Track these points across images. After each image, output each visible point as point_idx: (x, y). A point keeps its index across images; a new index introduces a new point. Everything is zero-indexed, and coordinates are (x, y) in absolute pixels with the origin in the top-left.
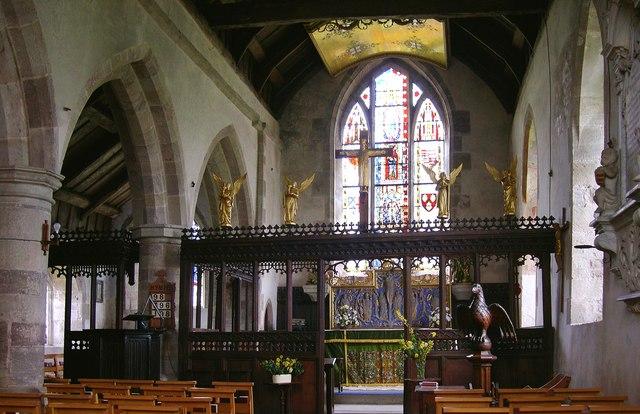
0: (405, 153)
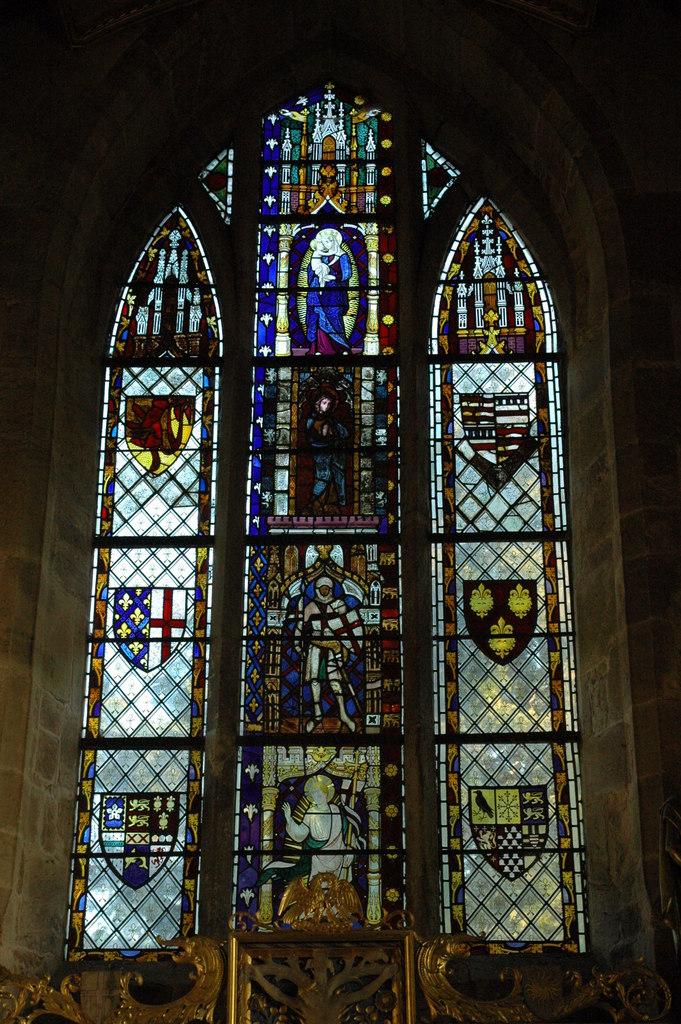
0: (383, 404)
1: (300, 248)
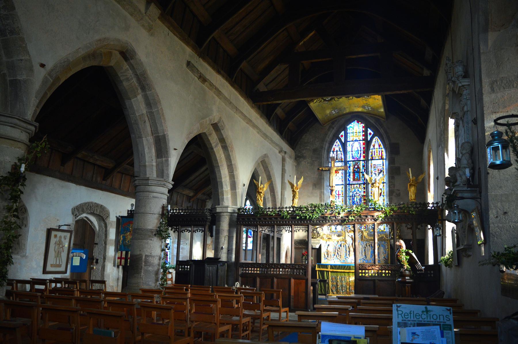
0: (364, 166)
1: (352, 146)
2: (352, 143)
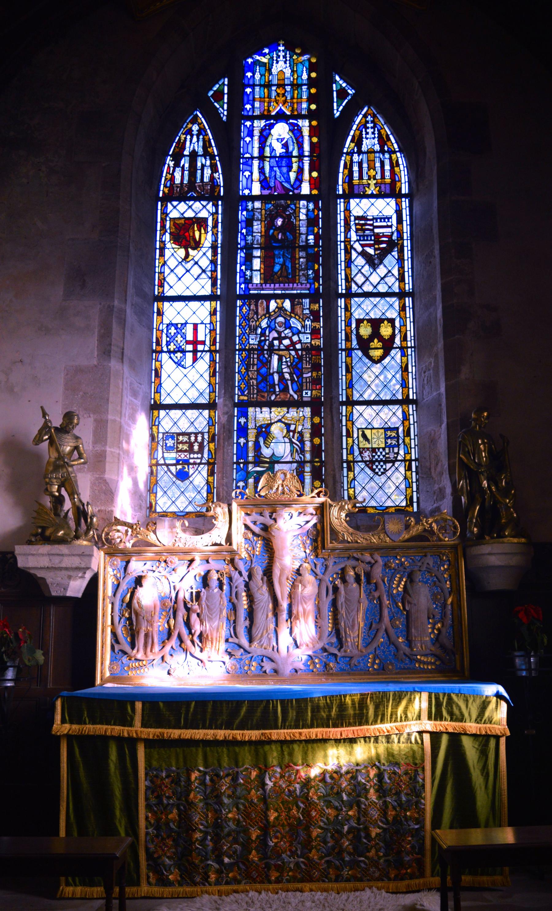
0: (312, 222)
2: (259, 124)
